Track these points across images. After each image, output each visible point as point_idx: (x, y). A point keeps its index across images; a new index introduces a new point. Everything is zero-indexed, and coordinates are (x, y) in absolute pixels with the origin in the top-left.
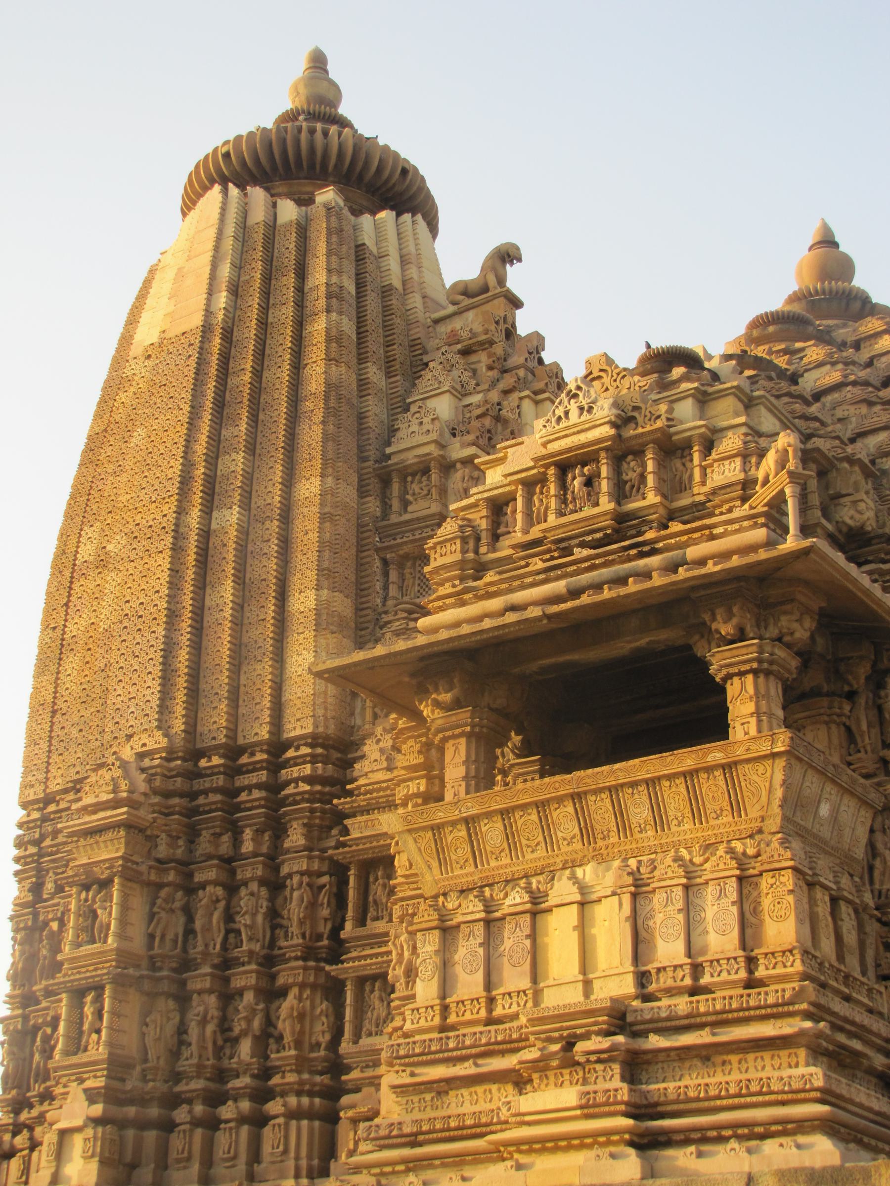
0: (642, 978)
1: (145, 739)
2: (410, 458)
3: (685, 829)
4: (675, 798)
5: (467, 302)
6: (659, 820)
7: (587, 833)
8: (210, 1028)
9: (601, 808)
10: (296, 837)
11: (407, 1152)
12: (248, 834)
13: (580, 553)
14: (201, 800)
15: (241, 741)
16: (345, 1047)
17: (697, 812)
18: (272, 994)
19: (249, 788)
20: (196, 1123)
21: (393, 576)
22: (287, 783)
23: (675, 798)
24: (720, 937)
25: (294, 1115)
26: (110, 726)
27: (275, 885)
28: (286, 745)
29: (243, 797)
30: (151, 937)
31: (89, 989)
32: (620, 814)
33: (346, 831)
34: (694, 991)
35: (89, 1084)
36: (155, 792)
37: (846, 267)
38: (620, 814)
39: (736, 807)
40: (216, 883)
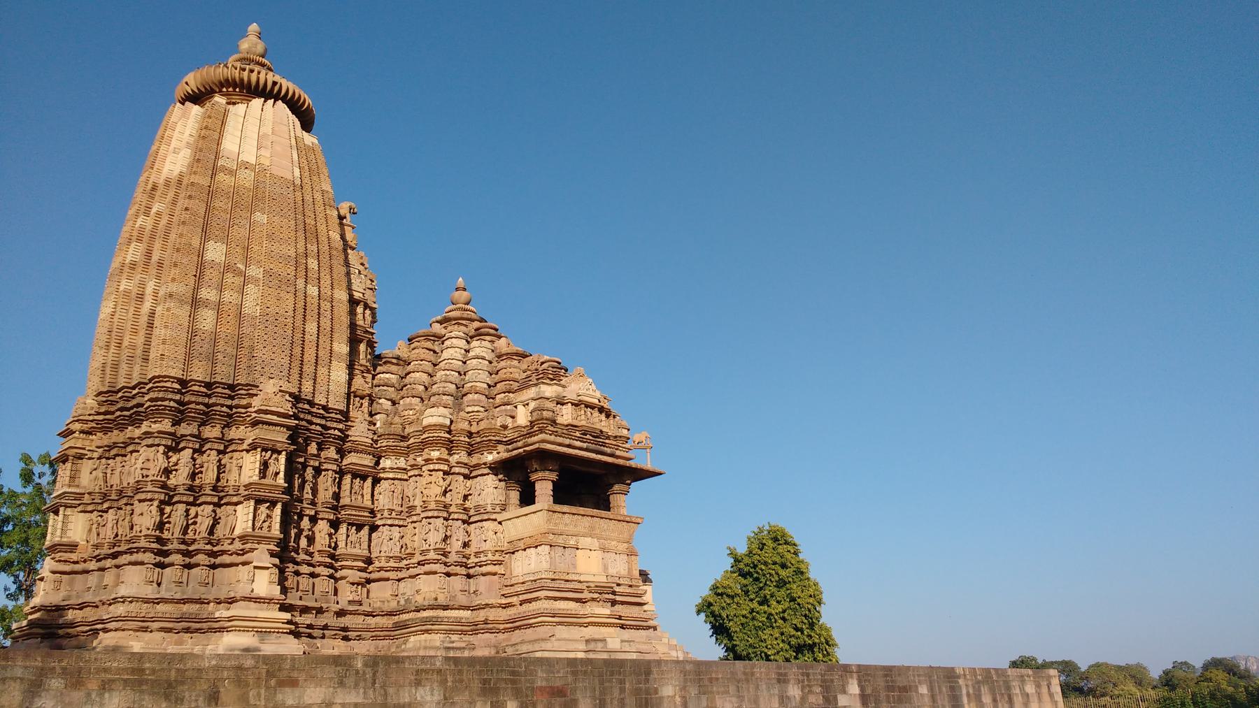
1: (281, 383)
35: (272, 547)
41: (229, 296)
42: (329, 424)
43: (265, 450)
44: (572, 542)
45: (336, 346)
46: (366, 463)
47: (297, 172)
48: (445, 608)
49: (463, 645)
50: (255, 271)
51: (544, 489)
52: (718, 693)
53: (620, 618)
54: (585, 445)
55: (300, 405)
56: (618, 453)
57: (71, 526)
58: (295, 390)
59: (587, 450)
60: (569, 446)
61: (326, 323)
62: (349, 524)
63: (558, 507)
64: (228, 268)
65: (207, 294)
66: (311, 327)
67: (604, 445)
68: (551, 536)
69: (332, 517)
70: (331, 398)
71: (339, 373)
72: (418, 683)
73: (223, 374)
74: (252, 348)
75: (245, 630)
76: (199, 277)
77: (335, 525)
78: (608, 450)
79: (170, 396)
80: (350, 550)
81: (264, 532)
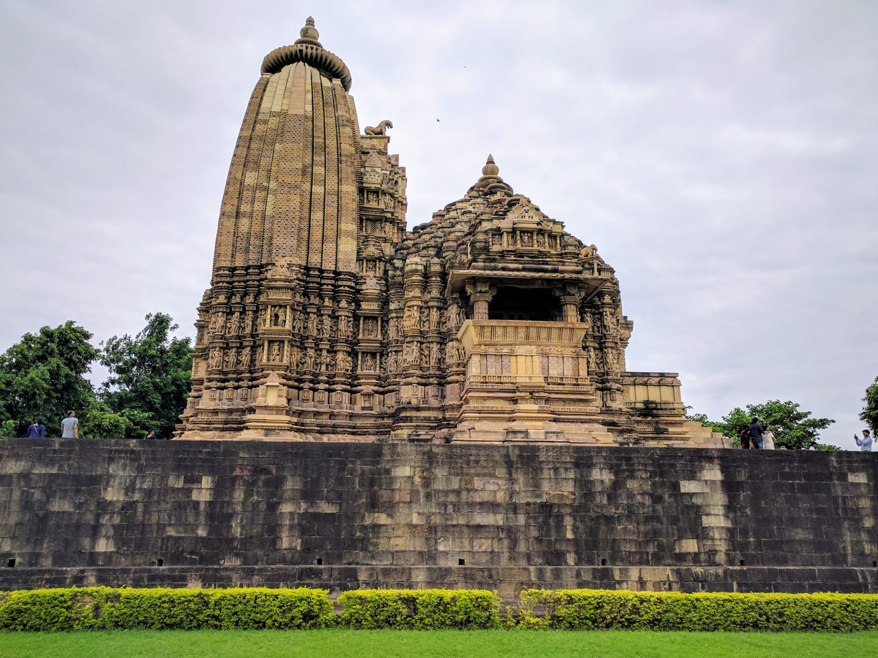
0: (546, 378)
1: (291, 259)
2: (373, 186)
3: (555, 341)
4: (555, 333)
5: (374, 135)
6: (549, 337)
7: (527, 337)
8: (313, 359)
9: (533, 331)
10: (343, 304)
11: (478, 415)
12: (326, 299)
13: (526, 258)
14: (311, 285)
15: (323, 268)
16: (359, 372)
17: (560, 337)
18: (332, 351)
19: (327, 285)
20: (311, 389)
21: (364, 224)
22: (340, 286)
23: (555, 333)
24: (569, 372)
25: (343, 390)
26: (274, 251)
27: (335, 317)
28: (339, 273)
29: (325, 287)
30: (294, 327)
31: (276, 341)
32: (538, 334)
33: (360, 306)
34: (559, 384)
36: (298, 279)
37: (495, 171)
38: (538, 334)
39: (571, 339)
40: (314, 313)
41: (258, 206)
42: (340, 283)
43: (275, 306)
44: (506, 350)
45: (343, 227)
46: (372, 308)
47: (309, 108)
48: (418, 409)
49: (429, 437)
50: (273, 185)
51: (481, 308)
52: (478, 475)
53: (553, 413)
54: (521, 266)
55: (311, 272)
56: (561, 268)
57: (199, 369)
58: (304, 263)
59: (524, 269)
60: (503, 269)
61: (332, 210)
62: (363, 353)
63: (494, 322)
64: (255, 189)
65: (245, 208)
66: (317, 216)
67: (546, 263)
68: (483, 347)
69: (349, 350)
70: (340, 264)
71: (348, 247)
72: (111, 460)
73: (253, 258)
74: (271, 238)
75: (256, 428)
76: (240, 198)
77: (353, 354)
78: (549, 267)
79: (223, 279)
80: (365, 372)
81: (277, 362)
